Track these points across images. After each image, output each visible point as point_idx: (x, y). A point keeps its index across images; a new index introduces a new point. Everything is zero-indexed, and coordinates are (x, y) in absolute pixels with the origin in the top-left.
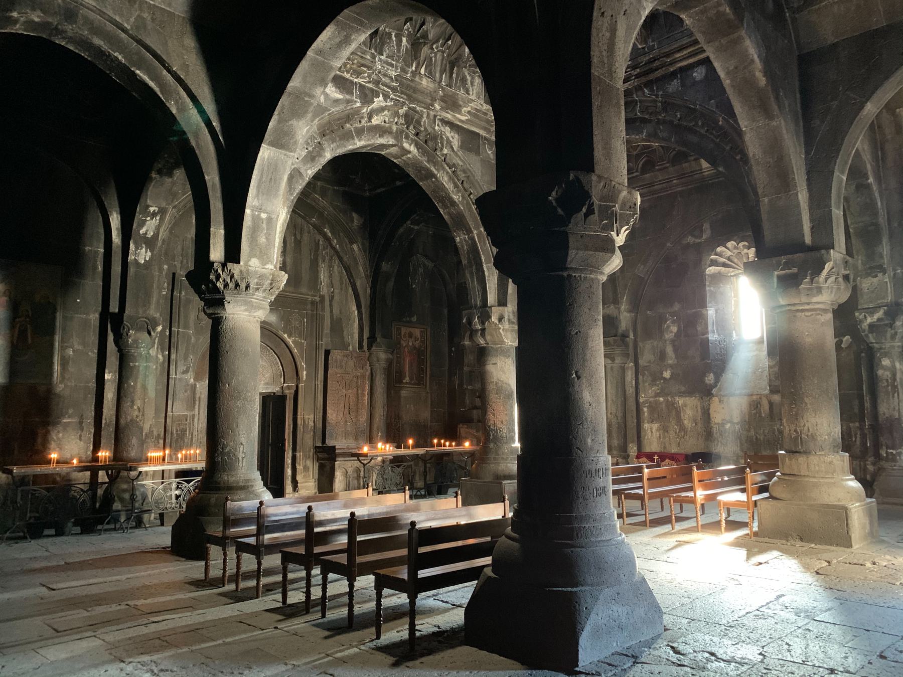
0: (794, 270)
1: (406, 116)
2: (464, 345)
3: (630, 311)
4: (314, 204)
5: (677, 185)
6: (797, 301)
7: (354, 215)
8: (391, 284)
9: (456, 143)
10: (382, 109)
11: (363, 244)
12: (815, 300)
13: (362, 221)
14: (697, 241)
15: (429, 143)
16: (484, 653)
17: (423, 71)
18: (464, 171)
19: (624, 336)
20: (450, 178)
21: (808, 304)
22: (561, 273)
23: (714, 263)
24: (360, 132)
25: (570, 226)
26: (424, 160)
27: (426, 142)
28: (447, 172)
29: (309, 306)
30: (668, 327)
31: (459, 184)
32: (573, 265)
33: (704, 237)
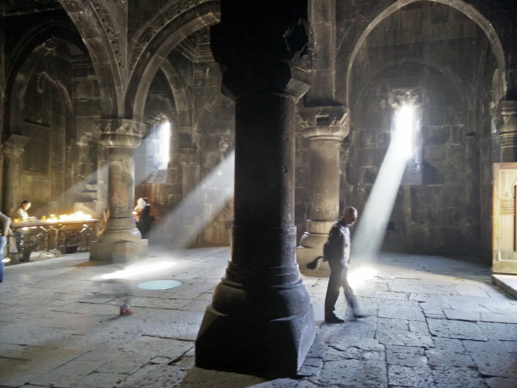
0: (327, 116)
2: (78, 146)
3: (199, 132)
6: (326, 134)
8: (23, 92)
12: (335, 134)
16: (223, 373)
19: (195, 148)
20: (95, 15)
21: (331, 136)
22: (278, 94)
25: (292, 60)
28: (93, 10)
30: (222, 144)
32: (287, 90)
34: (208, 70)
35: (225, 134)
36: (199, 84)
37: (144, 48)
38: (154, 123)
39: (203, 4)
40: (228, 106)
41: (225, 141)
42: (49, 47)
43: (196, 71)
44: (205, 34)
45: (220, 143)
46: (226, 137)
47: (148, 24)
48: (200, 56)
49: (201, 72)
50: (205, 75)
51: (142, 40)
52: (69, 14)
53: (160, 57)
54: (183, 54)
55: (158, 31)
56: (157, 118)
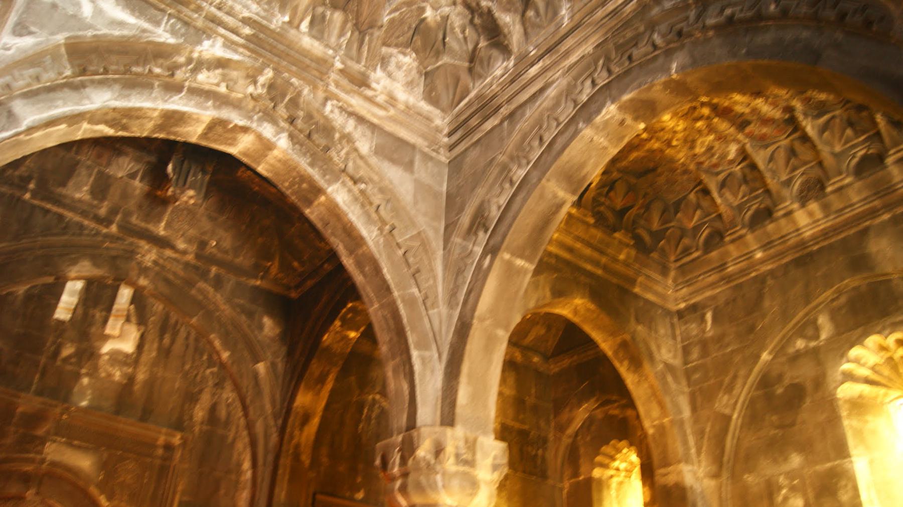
1: (271, 86)
4: (201, 297)
5: (763, 261)
7: (267, 322)
9: (364, 146)
10: (221, 64)
11: (273, 365)
13: (278, 331)
14: (813, 344)
15: (314, 135)
17: (304, 26)
18: (382, 190)
23: (849, 377)
24: (173, 88)
26: (304, 164)
27: (309, 136)
29: (160, 452)
30: (786, 499)
31: (372, 210)
33: (824, 336)
34: (709, 316)
35: (786, 467)
36: (695, 354)
37: (479, 250)
38: (612, 477)
39: (591, 99)
40: (780, 391)
41: (793, 489)
42: (351, 329)
43: (683, 328)
44: (681, 238)
45: (780, 499)
46: (791, 475)
47: (481, 192)
48: (685, 290)
49: (694, 326)
50: (704, 331)
51: (472, 231)
52: (307, 211)
53: (520, 262)
54: (637, 290)
55: (503, 200)
56: (616, 464)
